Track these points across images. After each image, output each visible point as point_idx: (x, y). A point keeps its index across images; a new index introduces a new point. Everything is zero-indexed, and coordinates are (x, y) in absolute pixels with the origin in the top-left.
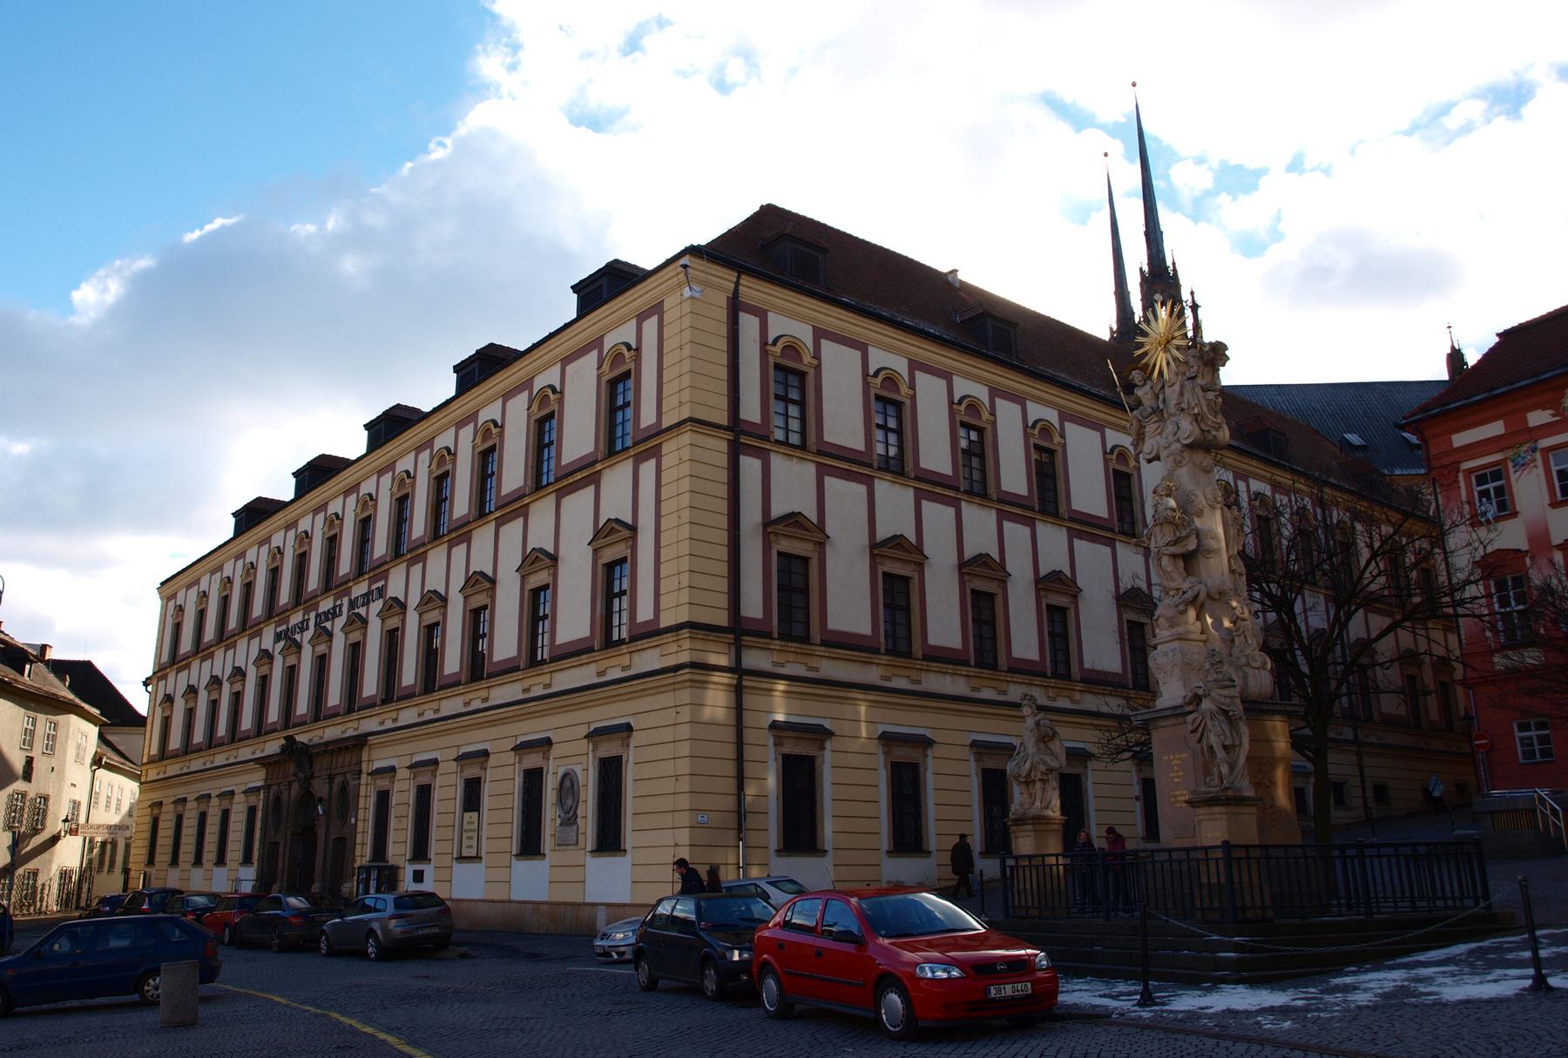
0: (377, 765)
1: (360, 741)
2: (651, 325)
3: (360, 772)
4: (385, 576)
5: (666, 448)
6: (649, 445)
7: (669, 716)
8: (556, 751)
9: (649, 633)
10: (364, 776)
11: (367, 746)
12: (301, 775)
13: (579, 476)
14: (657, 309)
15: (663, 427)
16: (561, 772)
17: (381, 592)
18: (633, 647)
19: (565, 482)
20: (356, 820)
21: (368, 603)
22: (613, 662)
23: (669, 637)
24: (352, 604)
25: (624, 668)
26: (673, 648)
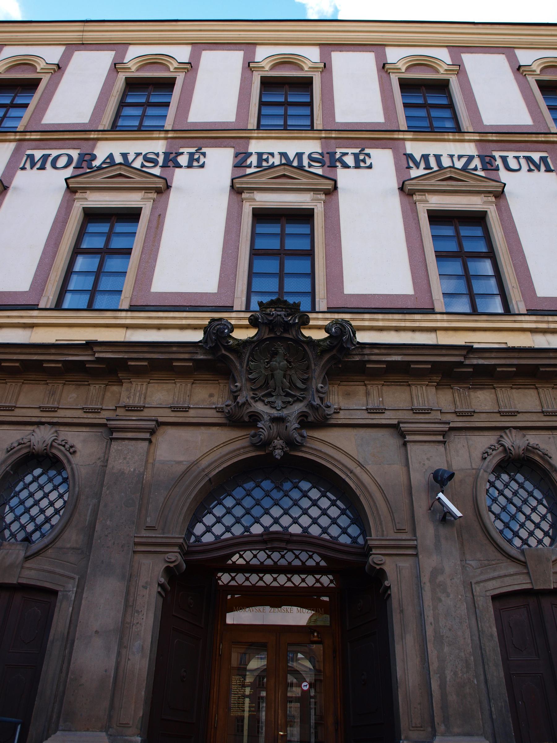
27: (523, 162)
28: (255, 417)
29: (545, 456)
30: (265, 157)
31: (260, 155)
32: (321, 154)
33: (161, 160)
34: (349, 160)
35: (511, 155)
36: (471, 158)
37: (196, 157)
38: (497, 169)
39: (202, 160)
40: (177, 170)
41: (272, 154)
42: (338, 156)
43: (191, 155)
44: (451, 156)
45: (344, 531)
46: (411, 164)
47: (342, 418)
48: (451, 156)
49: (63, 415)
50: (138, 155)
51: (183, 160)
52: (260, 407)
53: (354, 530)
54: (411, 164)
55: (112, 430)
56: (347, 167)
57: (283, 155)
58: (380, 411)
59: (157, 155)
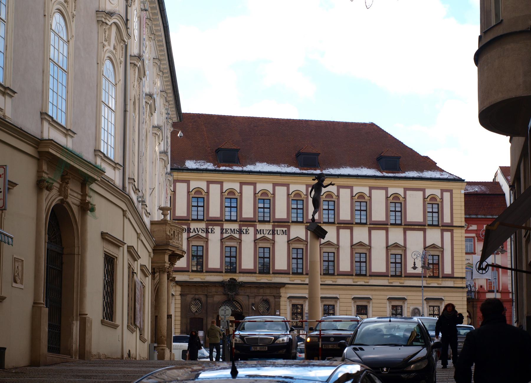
0: (289, 295)
1: (283, 285)
2: (447, 195)
3: (281, 296)
4: (289, 227)
5: (455, 231)
6: (449, 227)
7: (460, 299)
8: (408, 301)
9: (451, 277)
10: (282, 299)
11: (284, 288)
12: (229, 293)
13: (417, 227)
14: (451, 191)
15: (454, 225)
16: (412, 308)
17: (287, 233)
18: (444, 279)
19: (410, 227)
20: (280, 313)
21: (273, 234)
22: (434, 282)
23: (459, 280)
24: (256, 231)
25: (438, 284)
26: (461, 282)
27: (281, 231)
28: (228, 295)
29: (269, 300)
30: (227, 230)
31: (226, 229)
32: (239, 229)
33: (205, 230)
34: (245, 233)
35: (279, 229)
36: (270, 230)
37: (213, 229)
38: (275, 234)
39: (214, 231)
40: (209, 234)
41: (228, 229)
42: (242, 230)
43: (211, 229)
44: (266, 230)
45: (239, 310)
46: (257, 233)
47: (240, 294)
48: (266, 230)
49: (199, 293)
50: (200, 228)
51: (210, 230)
52: (229, 293)
53: (241, 309)
54: (257, 233)
55: (207, 296)
56: (244, 233)
57: (231, 229)
58: (245, 293)
59: (204, 229)
